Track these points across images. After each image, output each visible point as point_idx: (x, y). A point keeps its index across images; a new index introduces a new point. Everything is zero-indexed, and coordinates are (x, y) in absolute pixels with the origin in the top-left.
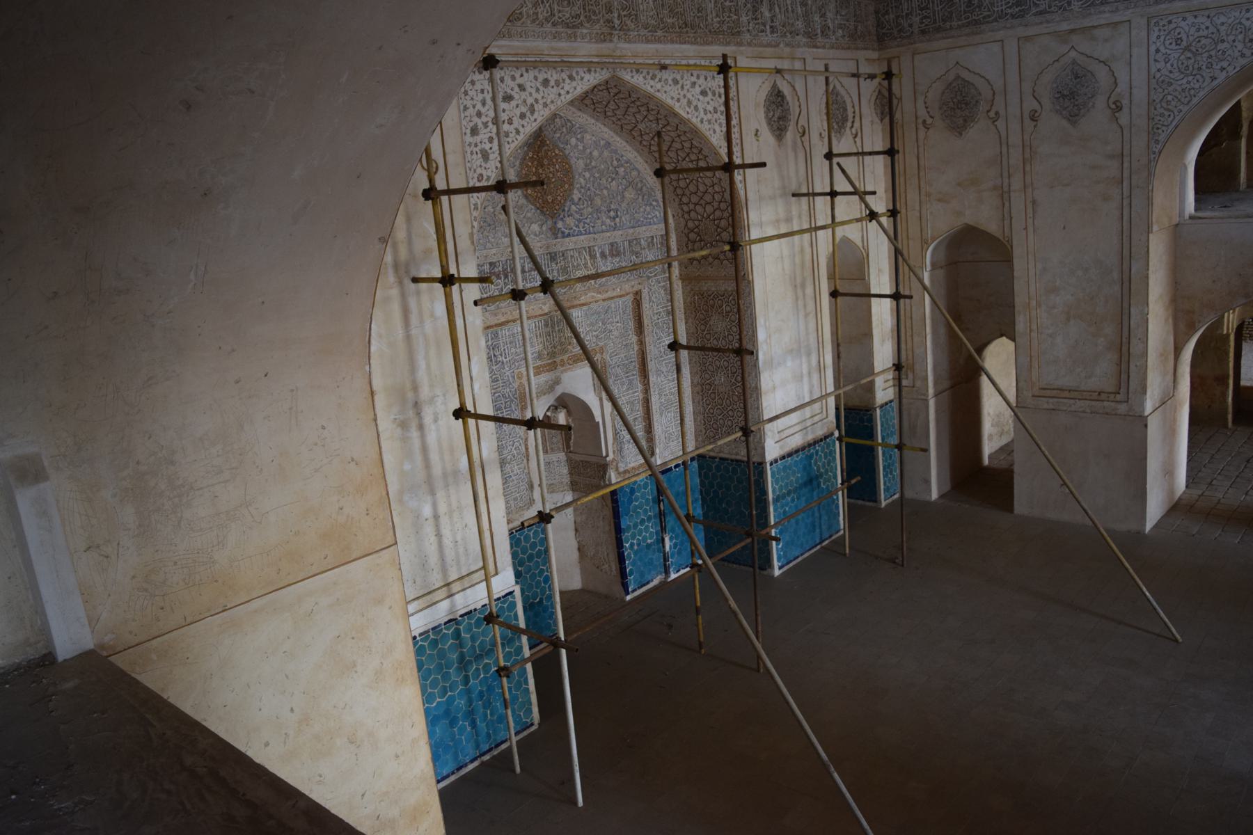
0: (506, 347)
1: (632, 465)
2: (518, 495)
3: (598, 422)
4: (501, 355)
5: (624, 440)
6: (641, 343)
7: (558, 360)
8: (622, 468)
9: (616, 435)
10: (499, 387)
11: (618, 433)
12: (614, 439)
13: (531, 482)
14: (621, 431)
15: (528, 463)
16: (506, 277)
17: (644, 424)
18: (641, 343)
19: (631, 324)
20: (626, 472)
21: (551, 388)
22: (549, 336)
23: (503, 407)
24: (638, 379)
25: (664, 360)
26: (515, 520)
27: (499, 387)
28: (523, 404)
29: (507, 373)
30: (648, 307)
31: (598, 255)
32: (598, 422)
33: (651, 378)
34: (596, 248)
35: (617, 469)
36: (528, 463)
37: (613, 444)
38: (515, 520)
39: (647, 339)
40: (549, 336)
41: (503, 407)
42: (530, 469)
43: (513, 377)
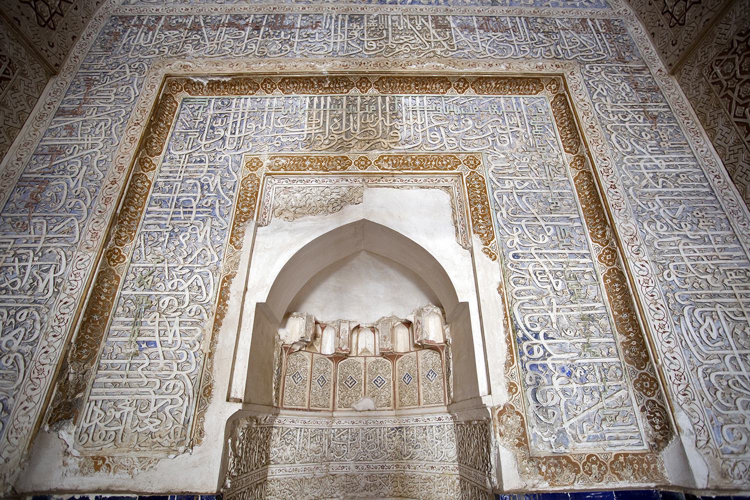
0: (239, 119)
1: (585, 447)
2: (153, 397)
3: (466, 305)
4: (226, 130)
5: (549, 362)
6: (582, 161)
7: (353, 154)
8: (543, 444)
9: (519, 341)
10: (202, 172)
11: (525, 338)
12: (511, 352)
13: (208, 378)
14: (537, 336)
15: (216, 330)
16: (257, 28)
17: (621, 338)
18: (582, 161)
19: (554, 135)
20: (560, 461)
21: (338, 205)
22: (340, 117)
23: (194, 204)
24: (588, 232)
25: (659, 193)
26: (122, 467)
27: (202, 172)
28: (245, 209)
29: (227, 154)
30: (587, 99)
31: (453, 25)
32: (466, 305)
33: (617, 221)
34: (450, 19)
35: (522, 442)
36: (216, 330)
37: (508, 364)
38: (122, 467)
39: (593, 149)
40: (340, 117)
41: (194, 204)
42: (218, 346)
43: (238, 163)
